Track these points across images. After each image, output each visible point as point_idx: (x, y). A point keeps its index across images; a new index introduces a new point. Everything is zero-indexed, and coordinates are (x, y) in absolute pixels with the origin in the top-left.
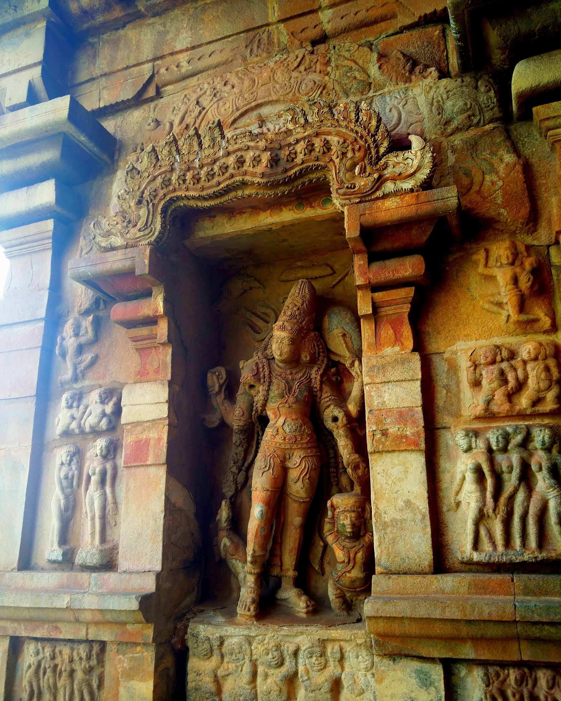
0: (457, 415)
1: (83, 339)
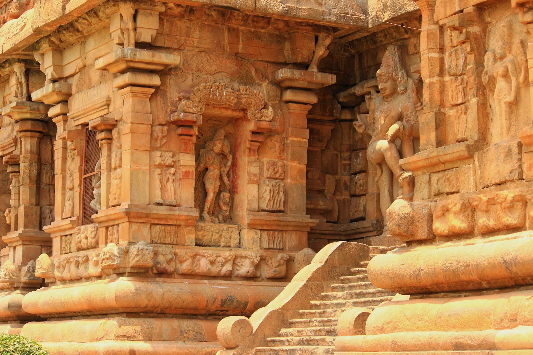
0: (263, 176)
1: (164, 134)
